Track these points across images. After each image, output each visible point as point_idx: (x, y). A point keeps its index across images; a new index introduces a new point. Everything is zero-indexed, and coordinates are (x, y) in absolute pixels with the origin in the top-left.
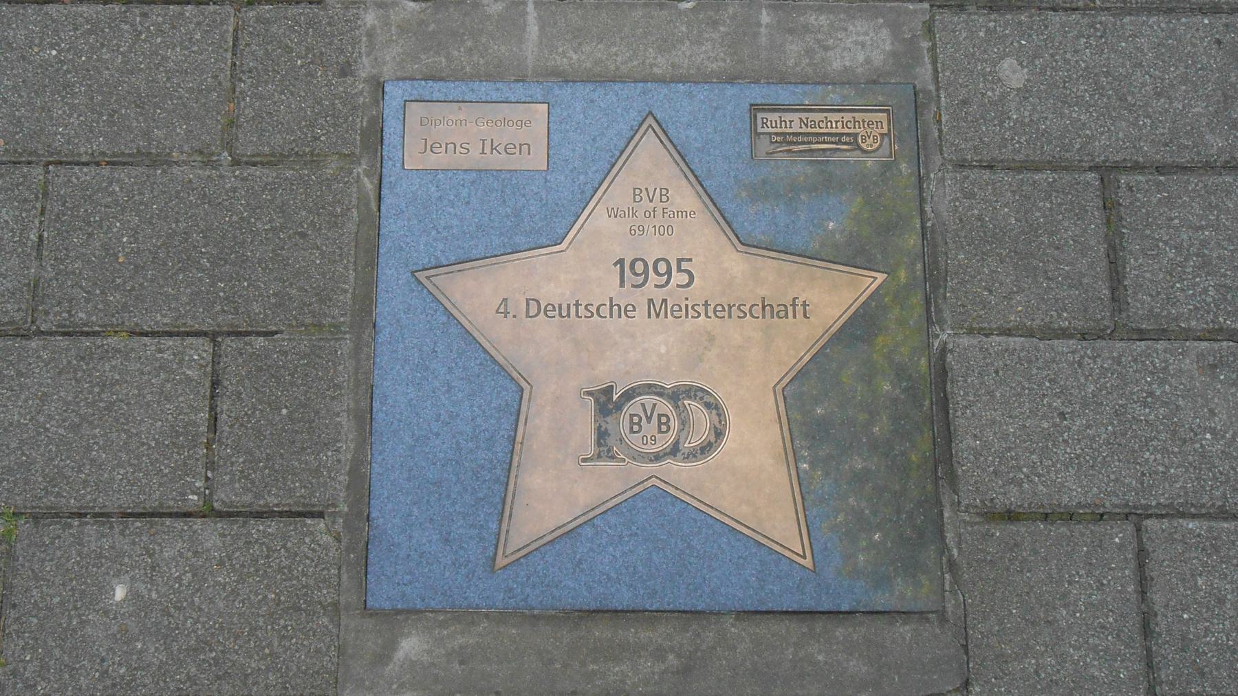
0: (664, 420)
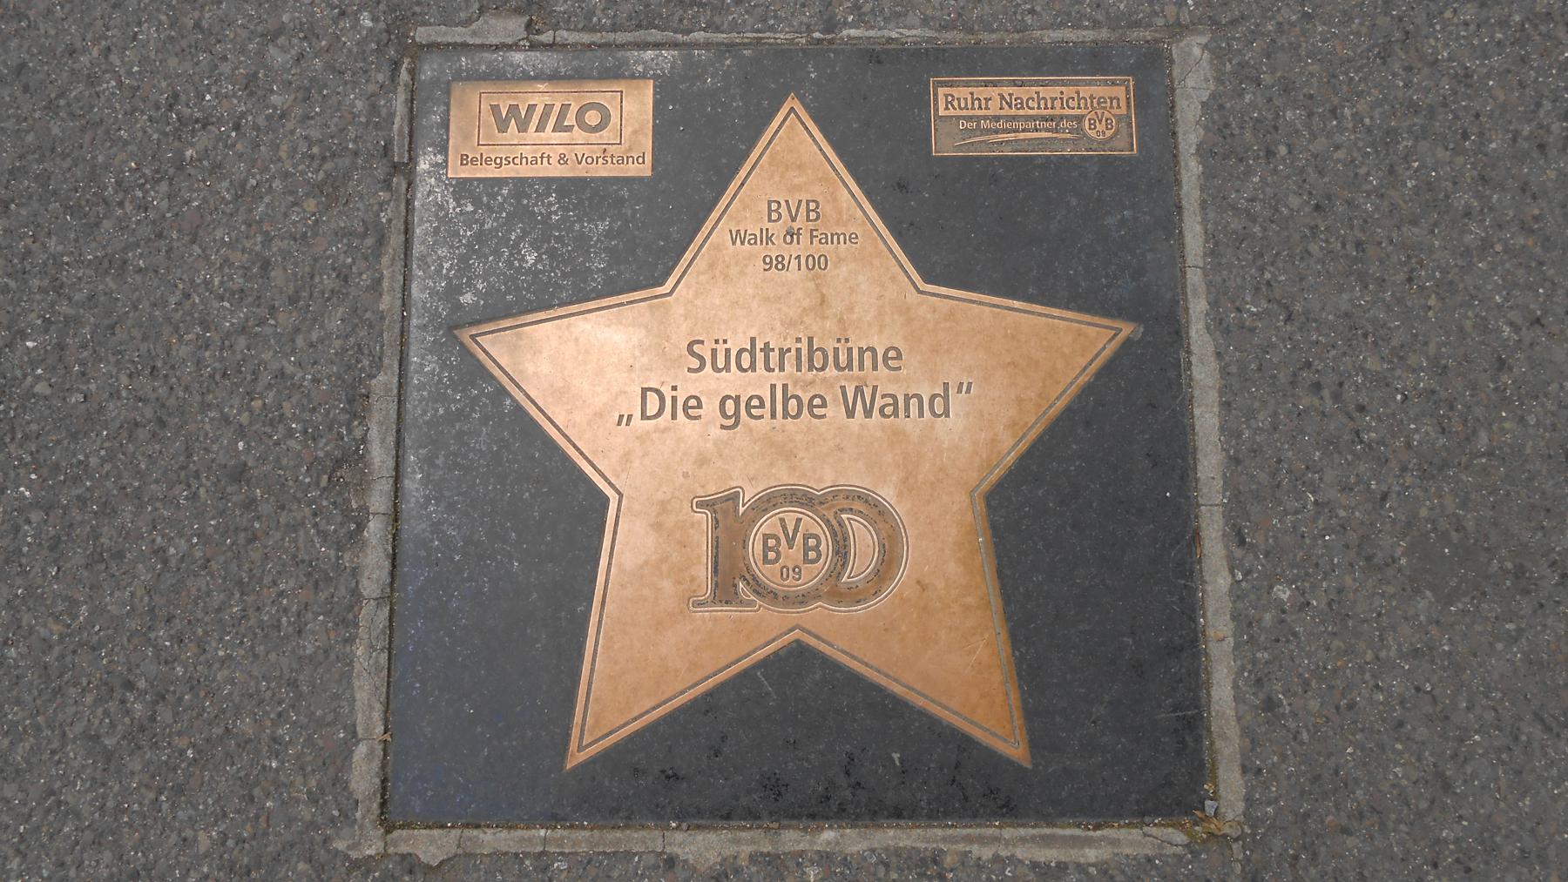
0: (812, 542)
